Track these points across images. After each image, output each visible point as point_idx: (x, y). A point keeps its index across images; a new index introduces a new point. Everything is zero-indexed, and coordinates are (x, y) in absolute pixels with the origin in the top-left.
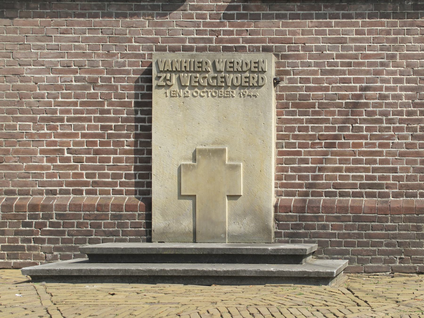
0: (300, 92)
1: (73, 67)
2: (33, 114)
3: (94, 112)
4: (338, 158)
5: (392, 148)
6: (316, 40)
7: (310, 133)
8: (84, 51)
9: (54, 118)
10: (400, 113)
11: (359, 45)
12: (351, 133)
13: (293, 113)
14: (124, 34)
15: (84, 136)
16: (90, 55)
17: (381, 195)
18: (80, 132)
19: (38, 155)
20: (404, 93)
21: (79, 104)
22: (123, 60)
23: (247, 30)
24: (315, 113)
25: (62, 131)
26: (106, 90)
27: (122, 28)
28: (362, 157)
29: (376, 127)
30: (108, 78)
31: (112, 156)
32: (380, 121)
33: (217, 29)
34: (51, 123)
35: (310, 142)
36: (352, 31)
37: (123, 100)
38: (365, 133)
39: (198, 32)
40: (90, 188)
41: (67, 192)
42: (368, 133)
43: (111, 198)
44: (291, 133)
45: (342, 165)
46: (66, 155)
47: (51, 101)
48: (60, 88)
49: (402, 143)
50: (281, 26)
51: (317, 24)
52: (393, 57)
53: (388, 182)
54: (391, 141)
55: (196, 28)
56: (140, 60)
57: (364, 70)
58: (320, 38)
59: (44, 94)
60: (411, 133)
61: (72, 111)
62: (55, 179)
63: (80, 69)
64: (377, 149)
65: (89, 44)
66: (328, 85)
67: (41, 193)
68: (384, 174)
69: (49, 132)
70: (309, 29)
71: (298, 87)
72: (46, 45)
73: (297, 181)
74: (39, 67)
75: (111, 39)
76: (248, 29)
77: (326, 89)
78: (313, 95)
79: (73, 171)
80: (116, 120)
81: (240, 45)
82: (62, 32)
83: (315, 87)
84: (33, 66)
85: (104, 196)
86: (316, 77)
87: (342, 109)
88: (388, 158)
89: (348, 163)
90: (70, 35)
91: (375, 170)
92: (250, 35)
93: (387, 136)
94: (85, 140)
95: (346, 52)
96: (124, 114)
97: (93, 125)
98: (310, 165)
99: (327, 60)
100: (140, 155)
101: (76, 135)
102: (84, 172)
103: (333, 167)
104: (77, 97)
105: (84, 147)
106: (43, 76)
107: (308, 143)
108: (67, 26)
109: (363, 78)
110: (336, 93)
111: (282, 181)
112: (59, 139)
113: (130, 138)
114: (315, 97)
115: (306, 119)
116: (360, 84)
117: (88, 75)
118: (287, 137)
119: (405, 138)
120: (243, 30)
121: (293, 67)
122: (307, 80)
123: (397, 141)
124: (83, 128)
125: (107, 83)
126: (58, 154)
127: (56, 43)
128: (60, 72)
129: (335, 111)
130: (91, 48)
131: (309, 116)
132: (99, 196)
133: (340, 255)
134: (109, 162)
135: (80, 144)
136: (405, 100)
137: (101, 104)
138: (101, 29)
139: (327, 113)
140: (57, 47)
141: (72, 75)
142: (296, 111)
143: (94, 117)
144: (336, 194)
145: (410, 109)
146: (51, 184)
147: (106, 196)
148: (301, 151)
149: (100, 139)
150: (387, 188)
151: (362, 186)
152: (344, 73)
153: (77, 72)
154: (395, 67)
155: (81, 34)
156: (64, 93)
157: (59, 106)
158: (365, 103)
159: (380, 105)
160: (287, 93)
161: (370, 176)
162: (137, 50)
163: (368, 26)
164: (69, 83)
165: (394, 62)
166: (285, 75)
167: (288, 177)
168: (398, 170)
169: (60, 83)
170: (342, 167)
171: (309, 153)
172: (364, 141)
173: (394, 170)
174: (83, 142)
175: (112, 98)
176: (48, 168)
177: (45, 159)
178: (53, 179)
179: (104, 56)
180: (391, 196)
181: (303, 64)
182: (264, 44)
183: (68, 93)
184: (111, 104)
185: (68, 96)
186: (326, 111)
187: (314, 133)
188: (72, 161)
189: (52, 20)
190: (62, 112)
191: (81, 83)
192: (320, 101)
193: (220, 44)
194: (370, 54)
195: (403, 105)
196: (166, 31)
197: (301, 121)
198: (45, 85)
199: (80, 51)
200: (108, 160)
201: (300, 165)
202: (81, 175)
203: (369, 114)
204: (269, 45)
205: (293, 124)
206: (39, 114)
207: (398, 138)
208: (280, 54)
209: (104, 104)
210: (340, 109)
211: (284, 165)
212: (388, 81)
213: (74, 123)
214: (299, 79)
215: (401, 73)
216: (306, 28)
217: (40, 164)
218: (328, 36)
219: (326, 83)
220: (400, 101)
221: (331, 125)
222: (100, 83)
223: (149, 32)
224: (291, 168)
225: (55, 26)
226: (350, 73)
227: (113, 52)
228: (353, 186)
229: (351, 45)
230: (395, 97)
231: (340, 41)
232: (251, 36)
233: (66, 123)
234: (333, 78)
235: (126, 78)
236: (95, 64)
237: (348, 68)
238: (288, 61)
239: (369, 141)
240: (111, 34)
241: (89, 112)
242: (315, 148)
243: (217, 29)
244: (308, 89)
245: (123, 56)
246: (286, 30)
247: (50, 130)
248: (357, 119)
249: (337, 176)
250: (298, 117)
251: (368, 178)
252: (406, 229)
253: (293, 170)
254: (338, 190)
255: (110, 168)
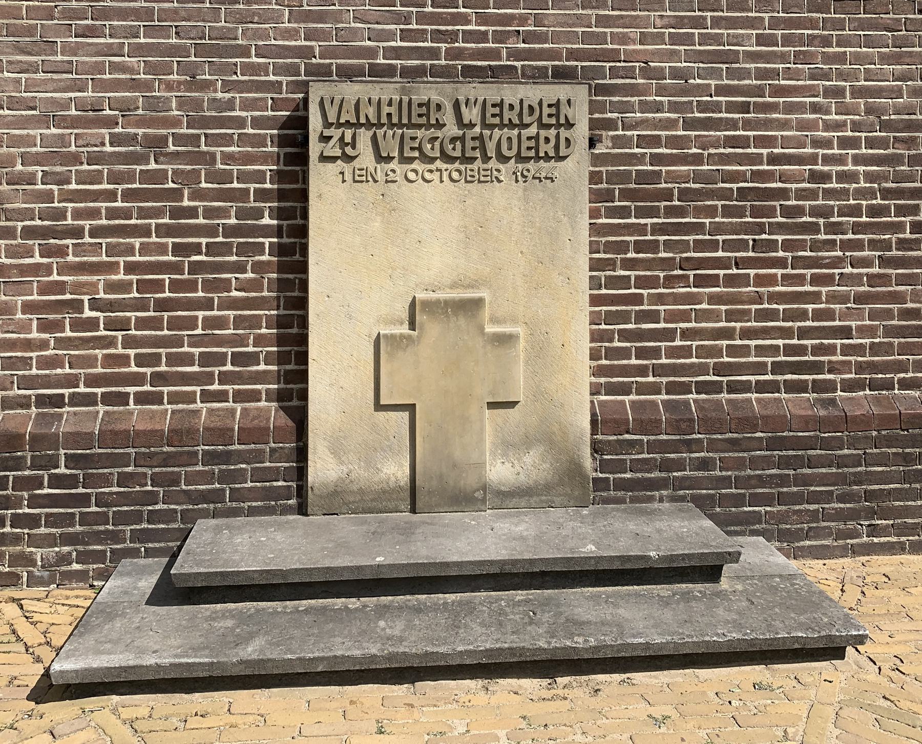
0: (637, 165)
1: (108, 112)
2: (7, 220)
3: (158, 213)
4: (723, 308)
5: (838, 285)
6: (672, 55)
7: (663, 255)
8: (134, 77)
9: (59, 228)
10: (855, 211)
11: (765, 68)
12: (751, 254)
13: (623, 212)
14: (231, 39)
15: (131, 268)
16: (148, 86)
17: (818, 386)
18: (121, 260)
19: (17, 316)
20: (861, 168)
21: (119, 196)
22: (227, 96)
23: (518, 32)
24: (671, 211)
25: (77, 259)
26: (187, 164)
27: (227, 25)
28: (775, 306)
29: (805, 240)
30: (193, 135)
31: (200, 314)
32: (813, 228)
33: (450, 28)
34: (52, 241)
35: (662, 275)
36: (749, 36)
37: (228, 186)
38: (781, 254)
39: (406, 35)
40: (147, 388)
41: (89, 400)
42: (787, 254)
43: (196, 412)
44: (619, 256)
45: (733, 324)
46: (88, 313)
47: (51, 189)
48: (75, 159)
49: (861, 275)
50: (594, 23)
51: (672, 22)
52: (838, 92)
53: (834, 358)
54: (837, 271)
55: (402, 27)
56: (269, 96)
57: (777, 120)
58: (680, 51)
59: (34, 174)
60: (879, 253)
61: (103, 211)
62: (59, 371)
63: (122, 116)
64: (808, 288)
65: (145, 59)
66: (700, 151)
67: (24, 403)
68: (823, 341)
69: (45, 260)
70: (656, 30)
71: (634, 155)
72: (40, 63)
73: (634, 361)
74: (24, 113)
75: (201, 50)
76: (521, 29)
77: (697, 160)
78: (667, 172)
79: (105, 352)
80: (211, 231)
81: (502, 63)
82: (80, 32)
83: (671, 154)
84: (8, 109)
85: (180, 406)
86: (674, 133)
87: (731, 203)
88: (832, 306)
89: (746, 318)
90: (102, 40)
91: (804, 333)
92: (524, 42)
93: (827, 261)
94: (134, 278)
95: (736, 82)
96: (229, 217)
97: (155, 243)
98: (662, 325)
99: (697, 99)
100: (269, 310)
101: (111, 267)
102: (132, 352)
103: (713, 329)
104: (115, 178)
105: (131, 296)
106: (31, 132)
107: (658, 277)
108: (92, 19)
109: (776, 137)
110: (718, 168)
111: (600, 362)
112: (71, 278)
113: (245, 271)
114: (673, 177)
115: (653, 224)
116: (770, 150)
117: (144, 130)
118: (610, 265)
119: (866, 263)
120: (509, 31)
121: (622, 113)
122: (655, 141)
123: (849, 270)
124: (130, 250)
125: (190, 149)
126: (68, 313)
127: (66, 58)
128: (74, 123)
129: (716, 206)
130: (151, 68)
131: (660, 217)
132: (169, 406)
133: (741, 524)
134: (195, 327)
135: (123, 287)
136: (865, 183)
137: (176, 194)
138: (176, 27)
139: (698, 212)
140: (67, 67)
141: (103, 131)
142: (630, 207)
143: (157, 225)
144: (722, 387)
145: (874, 202)
146: (47, 382)
147: (185, 406)
148: (642, 295)
149: (172, 276)
150: (830, 372)
151: (778, 368)
152: (733, 124)
153: (117, 124)
154: (842, 114)
155: (127, 37)
156: (85, 171)
157: (71, 201)
158: (780, 189)
159: (812, 194)
160: (610, 168)
161: (794, 345)
162: (262, 73)
163: (782, 26)
164: (96, 149)
165: (839, 104)
166: (605, 130)
167: (612, 353)
168: (854, 333)
169: (73, 148)
170: (734, 328)
171: (660, 299)
172: (779, 272)
173: (846, 332)
174: (130, 283)
175: (200, 182)
176: (44, 345)
177: (35, 323)
178: (54, 372)
179: (182, 87)
180: (839, 388)
181: (645, 107)
182: (557, 63)
183: (94, 171)
184: (197, 195)
185: (95, 178)
186: (695, 207)
187: (671, 255)
188: (102, 326)
189: (56, 6)
190: (77, 214)
191: (126, 149)
192: (683, 185)
193: (457, 62)
194: (790, 86)
195: (861, 193)
196: (330, 33)
197: (640, 229)
198: (37, 153)
199: (123, 76)
200: (191, 323)
201: (639, 326)
202: (123, 360)
203: (788, 212)
204: (567, 63)
205: (624, 235)
206: (22, 221)
207: (851, 264)
208: (593, 83)
209: (182, 196)
210: (727, 203)
211: (603, 327)
212: (827, 144)
213: (108, 240)
214: (635, 138)
215: (856, 127)
216: (650, 30)
217: (22, 336)
218: (698, 47)
219: (695, 147)
220: (854, 185)
221: (708, 237)
222: (172, 148)
223: (291, 34)
224: (620, 331)
225: (64, 18)
226: (748, 124)
227: (204, 77)
228: (759, 368)
229: (748, 66)
230: (843, 177)
231: (724, 58)
232: (527, 46)
233: (87, 240)
234: (710, 136)
235: (236, 137)
236: (160, 105)
237: (741, 115)
238: (611, 98)
239: (789, 271)
240: (201, 39)
241: (144, 213)
242: (674, 288)
243: (450, 28)
244: (657, 159)
245: (228, 86)
246: (605, 33)
247: (49, 257)
248: (764, 223)
249: (722, 349)
250: (633, 220)
251: (790, 350)
252: (882, 460)
253: (625, 335)
254: (725, 379)
255: (196, 341)
